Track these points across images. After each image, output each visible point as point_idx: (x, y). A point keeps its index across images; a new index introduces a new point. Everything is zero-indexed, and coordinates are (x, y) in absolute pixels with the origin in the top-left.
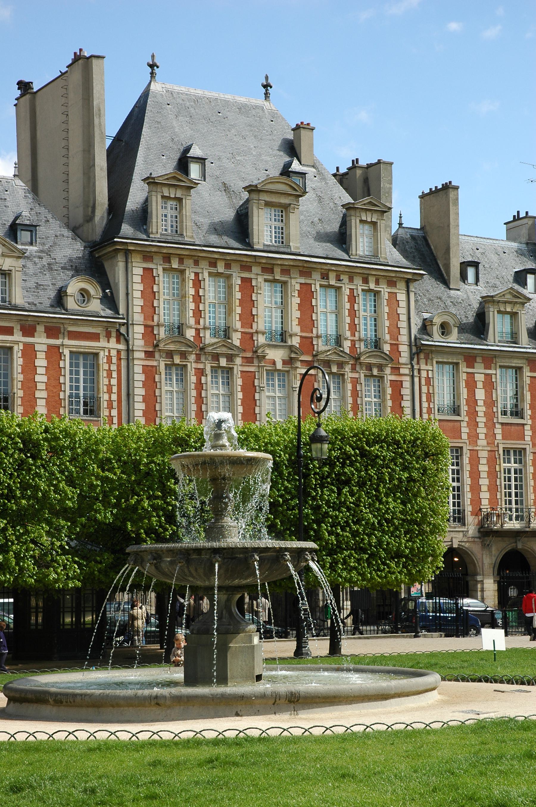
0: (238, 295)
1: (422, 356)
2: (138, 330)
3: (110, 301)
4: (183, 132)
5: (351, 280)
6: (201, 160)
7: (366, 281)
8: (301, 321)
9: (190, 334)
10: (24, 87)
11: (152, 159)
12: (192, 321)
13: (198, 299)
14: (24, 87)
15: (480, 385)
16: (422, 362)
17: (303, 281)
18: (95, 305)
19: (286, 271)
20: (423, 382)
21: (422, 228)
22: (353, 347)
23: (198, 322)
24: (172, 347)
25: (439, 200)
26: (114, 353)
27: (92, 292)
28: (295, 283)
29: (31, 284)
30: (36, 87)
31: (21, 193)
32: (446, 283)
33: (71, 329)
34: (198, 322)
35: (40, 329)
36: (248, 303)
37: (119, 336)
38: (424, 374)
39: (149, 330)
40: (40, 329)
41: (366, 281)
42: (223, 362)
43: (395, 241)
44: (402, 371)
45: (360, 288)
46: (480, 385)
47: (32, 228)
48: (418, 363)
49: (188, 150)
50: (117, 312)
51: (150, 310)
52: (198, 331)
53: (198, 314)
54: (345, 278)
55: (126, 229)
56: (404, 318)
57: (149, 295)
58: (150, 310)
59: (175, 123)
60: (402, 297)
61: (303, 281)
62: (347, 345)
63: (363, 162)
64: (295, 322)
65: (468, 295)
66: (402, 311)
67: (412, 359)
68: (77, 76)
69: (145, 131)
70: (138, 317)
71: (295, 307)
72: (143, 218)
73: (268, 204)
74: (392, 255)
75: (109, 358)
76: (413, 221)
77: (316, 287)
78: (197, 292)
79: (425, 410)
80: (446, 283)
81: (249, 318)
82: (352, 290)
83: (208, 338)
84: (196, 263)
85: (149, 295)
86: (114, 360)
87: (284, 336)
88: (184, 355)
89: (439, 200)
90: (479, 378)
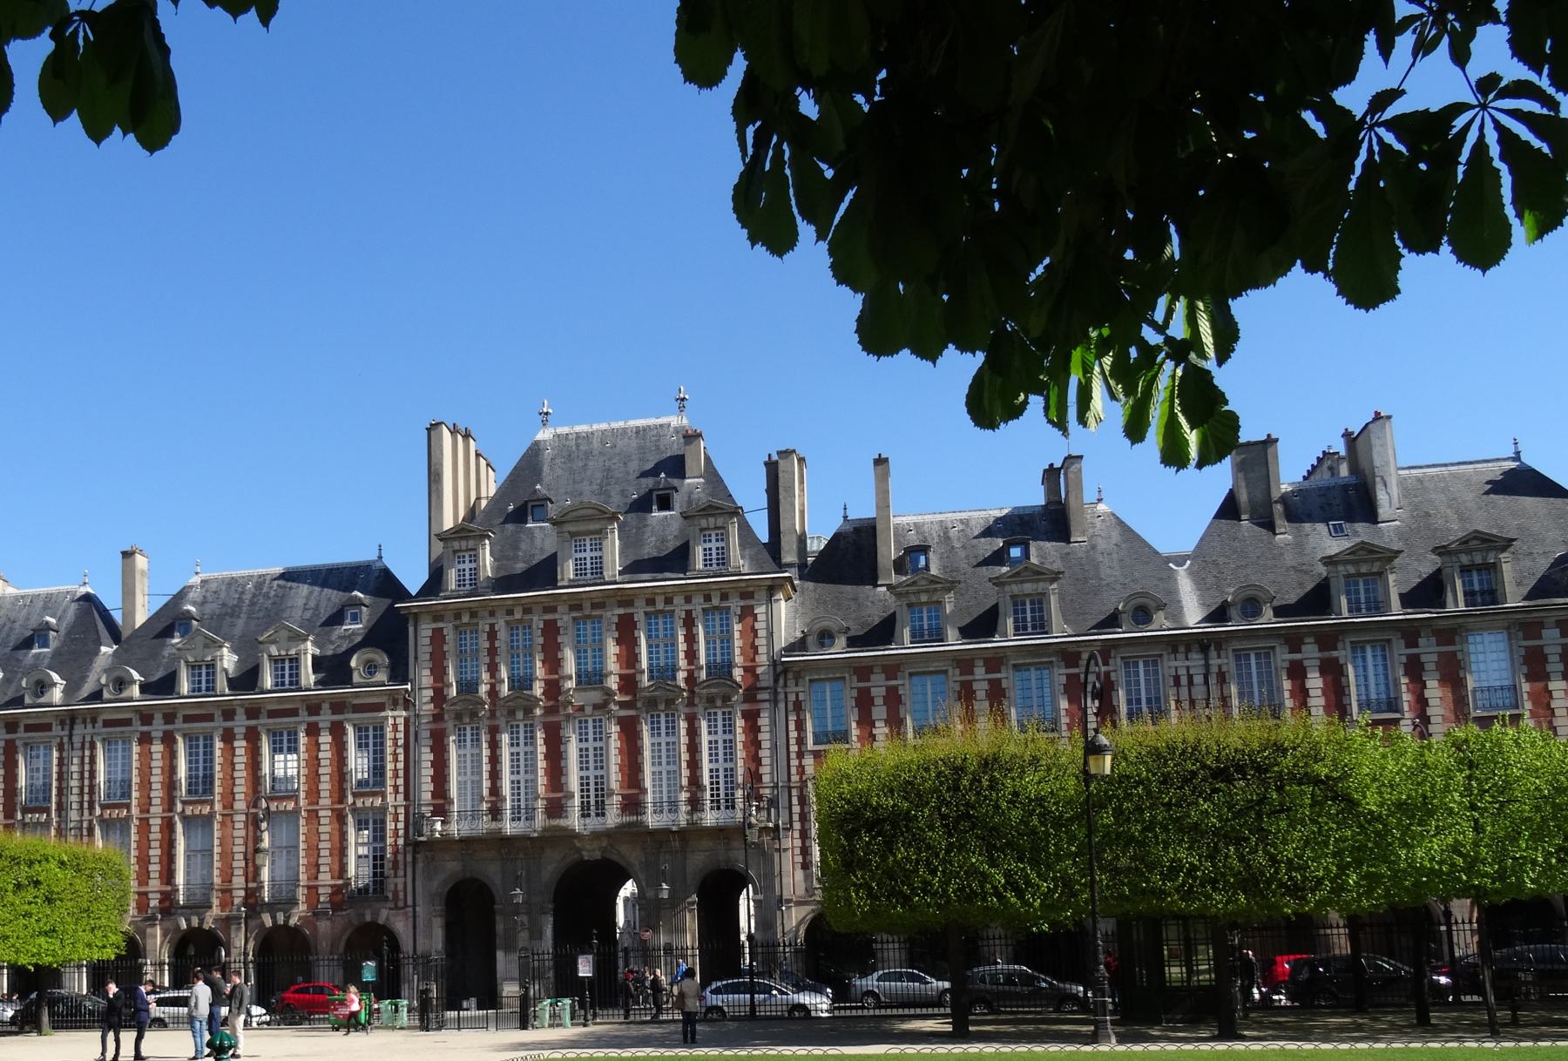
1: (790, 675)
5: (688, 600)
7: (708, 598)
15: (879, 701)
16: (791, 683)
17: (621, 611)
20: (791, 707)
26: (401, 721)
33: (356, 702)
35: (326, 706)
37: (407, 705)
38: (792, 698)
40: (326, 706)
41: (708, 598)
44: (759, 697)
45: (699, 608)
46: (879, 701)
48: (785, 686)
54: (679, 600)
61: (621, 611)
67: (776, 681)
75: (395, 726)
77: (639, 617)
78: (492, 644)
79: (793, 741)
82: (689, 613)
84: (492, 614)
86: (401, 728)
90: (878, 692)
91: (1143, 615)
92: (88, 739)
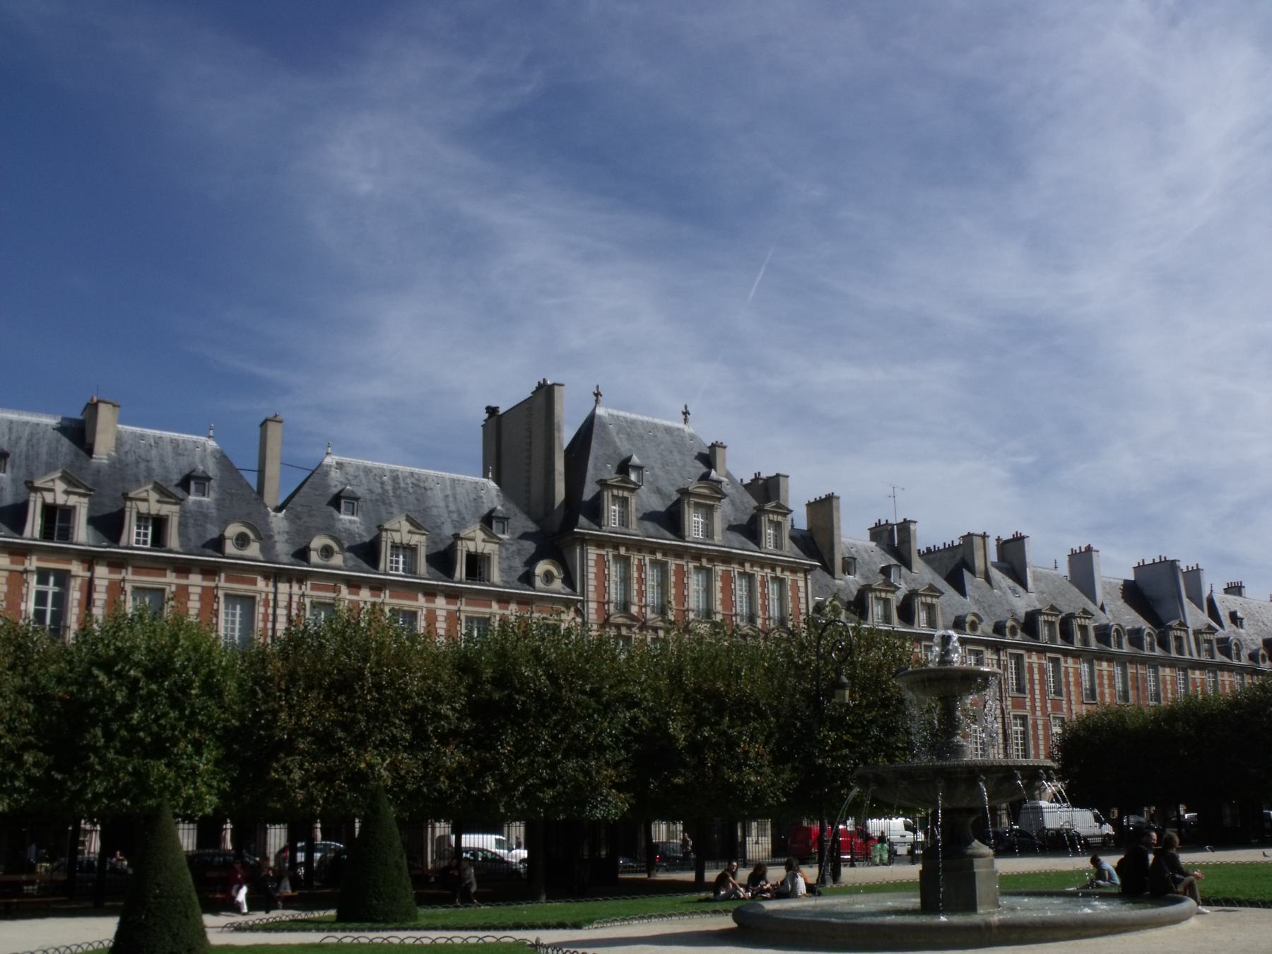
0: (673, 579)
2: (593, 606)
3: (569, 581)
4: (624, 447)
6: (639, 468)
8: (723, 602)
9: (634, 610)
10: (492, 411)
11: (598, 468)
12: (636, 600)
13: (641, 581)
14: (492, 411)
18: (558, 584)
19: (710, 560)
21: (810, 530)
22: (764, 623)
23: (641, 600)
24: (620, 621)
25: (823, 508)
27: (555, 572)
28: (720, 568)
29: (505, 565)
30: (501, 411)
31: (494, 493)
32: (831, 573)
34: (641, 600)
36: (682, 585)
37: (579, 612)
39: (602, 604)
42: (661, 634)
43: (792, 538)
47: (503, 520)
49: (629, 459)
50: (574, 589)
51: (602, 588)
52: (641, 607)
53: (641, 594)
55: (582, 520)
56: (803, 600)
57: (603, 578)
58: (602, 588)
59: (617, 440)
60: (801, 584)
62: (759, 622)
63: (764, 475)
64: (718, 602)
65: (850, 583)
66: (802, 595)
68: (541, 400)
69: (594, 444)
70: (592, 595)
71: (718, 589)
72: (595, 511)
73: (697, 505)
74: (790, 551)
76: (802, 522)
80: (831, 573)
81: (682, 598)
83: (650, 615)
85: (603, 578)
87: (709, 613)
88: (629, 627)
89: (823, 508)
91: (974, 626)
92: (295, 599)
